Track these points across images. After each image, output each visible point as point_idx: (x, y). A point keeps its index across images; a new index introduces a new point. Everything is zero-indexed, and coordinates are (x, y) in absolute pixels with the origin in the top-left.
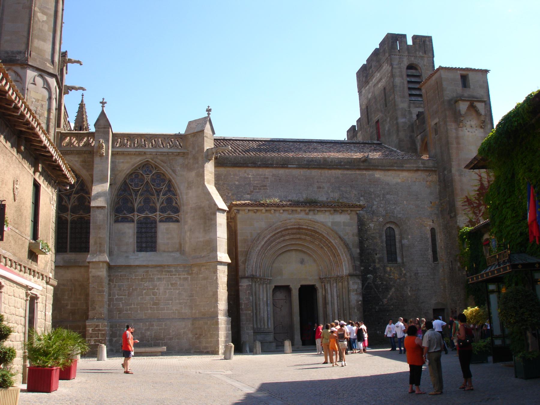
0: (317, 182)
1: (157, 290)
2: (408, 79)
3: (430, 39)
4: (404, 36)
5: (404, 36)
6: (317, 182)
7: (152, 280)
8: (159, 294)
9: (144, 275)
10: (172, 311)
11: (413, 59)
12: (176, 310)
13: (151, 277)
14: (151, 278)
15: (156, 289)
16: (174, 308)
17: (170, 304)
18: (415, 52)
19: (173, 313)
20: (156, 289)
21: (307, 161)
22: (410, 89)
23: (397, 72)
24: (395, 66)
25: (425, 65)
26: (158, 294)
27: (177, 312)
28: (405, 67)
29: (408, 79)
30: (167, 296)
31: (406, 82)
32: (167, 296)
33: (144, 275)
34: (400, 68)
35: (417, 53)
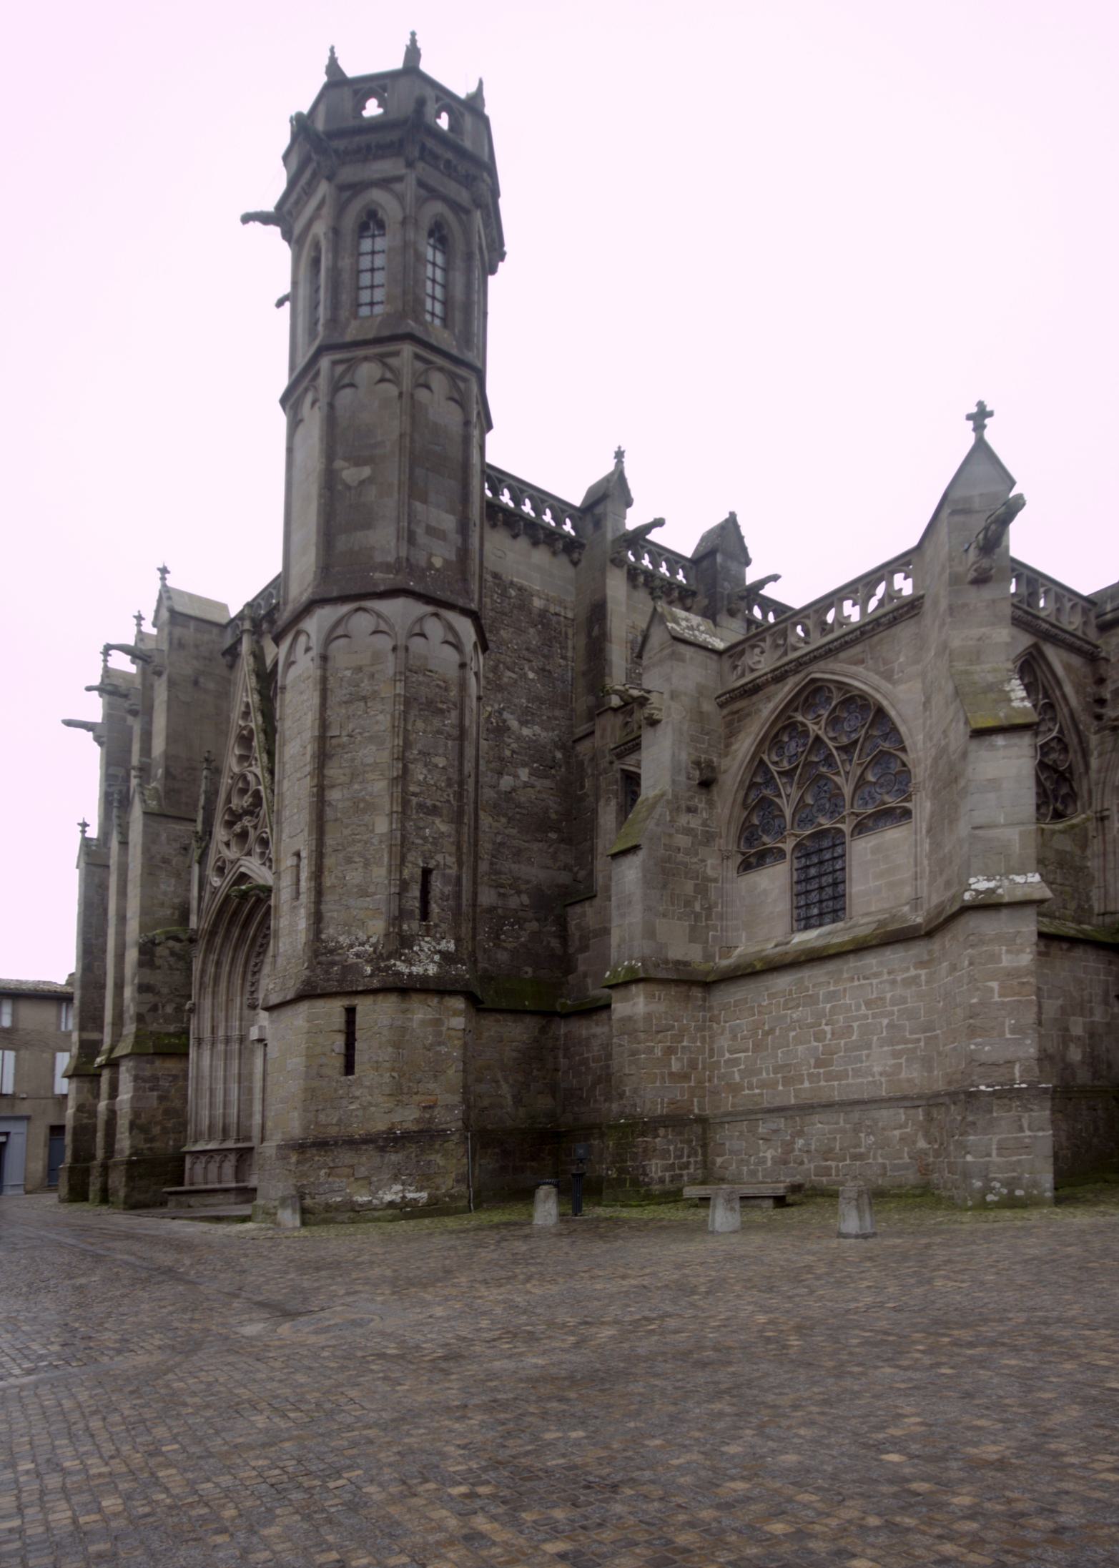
1: (826, 1025)
7: (813, 1000)
8: (833, 1034)
9: (791, 990)
10: (870, 1079)
12: (881, 1074)
13: (810, 992)
14: (811, 996)
15: (824, 1022)
16: (877, 1069)
17: (864, 1058)
19: (874, 1082)
20: (824, 1022)
26: (829, 1036)
27: (883, 1079)
30: (854, 1038)
32: (854, 1038)
33: (791, 990)
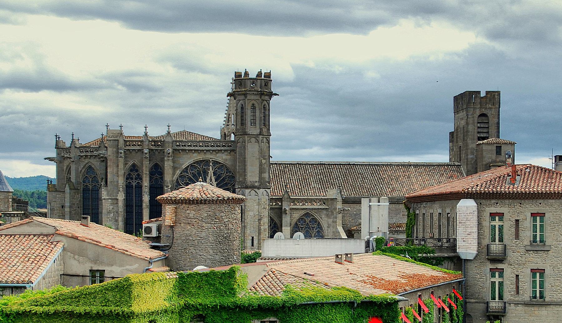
0: (403, 212)
2: (479, 125)
3: (498, 93)
4: (479, 92)
5: (479, 92)
6: (403, 212)
11: (483, 110)
18: (486, 105)
21: (397, 199)
22: (478, 132)
23: (470, 121)
24: (469, 116)
25: (492, 114)
28: (477, 117)
29: (479, 125)
31: (476, 128)
34: (473, 117)
35: (487, 105)
